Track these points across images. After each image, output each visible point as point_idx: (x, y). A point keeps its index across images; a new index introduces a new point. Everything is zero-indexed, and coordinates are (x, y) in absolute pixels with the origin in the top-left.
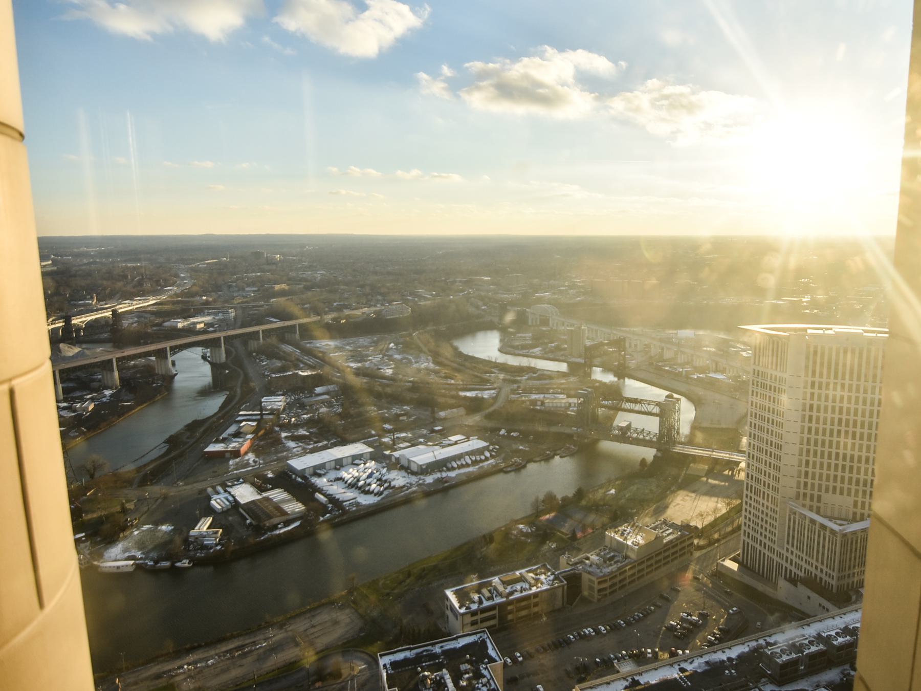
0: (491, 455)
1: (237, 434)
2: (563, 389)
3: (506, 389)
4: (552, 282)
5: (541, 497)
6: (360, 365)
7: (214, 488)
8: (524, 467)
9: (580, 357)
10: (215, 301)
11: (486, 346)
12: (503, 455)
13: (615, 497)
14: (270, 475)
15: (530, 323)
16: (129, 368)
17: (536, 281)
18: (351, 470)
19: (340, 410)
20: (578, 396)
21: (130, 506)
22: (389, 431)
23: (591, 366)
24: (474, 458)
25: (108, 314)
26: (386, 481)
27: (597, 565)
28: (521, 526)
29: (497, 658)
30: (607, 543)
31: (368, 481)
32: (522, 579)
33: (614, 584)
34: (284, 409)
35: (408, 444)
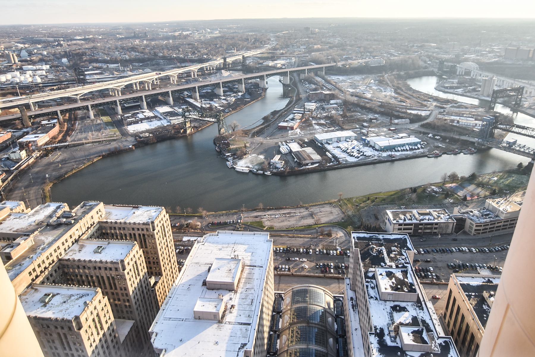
0: (421, 147)
1: (293, 119)
2: (474, 115)
3: (437, 111)
4: (477, 48)
5: (448, 174)
6: (354, 90)
7: (282, 142)
8: (440, 156)
9: (488, 96)
10: (286, 53)
11: (427, 86)
12: (428, 148)
13: (496, 182)
14: (306, 140)
15: (458, 73)
16: (248, 83)
17: (466, 47)
18: (344, 144)
19: (342, 113)
20: (483, 120)
21: (248, 145)
22: (366, 127)
23: (495, 104)
24: (411, 147)
25: (241, 57)
26: (361, 152)
27: (477, 216)
28: (433, 187)
29: (412, 249)
30: (486, 205)
31: (353, 150)
32: (429, 214)
33: (487, 229)
34: (315, 110)
35: (375, 135)
